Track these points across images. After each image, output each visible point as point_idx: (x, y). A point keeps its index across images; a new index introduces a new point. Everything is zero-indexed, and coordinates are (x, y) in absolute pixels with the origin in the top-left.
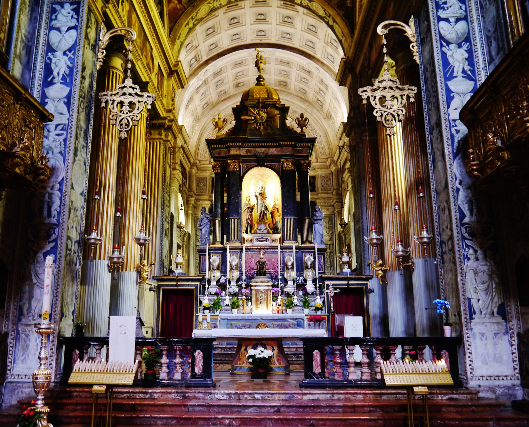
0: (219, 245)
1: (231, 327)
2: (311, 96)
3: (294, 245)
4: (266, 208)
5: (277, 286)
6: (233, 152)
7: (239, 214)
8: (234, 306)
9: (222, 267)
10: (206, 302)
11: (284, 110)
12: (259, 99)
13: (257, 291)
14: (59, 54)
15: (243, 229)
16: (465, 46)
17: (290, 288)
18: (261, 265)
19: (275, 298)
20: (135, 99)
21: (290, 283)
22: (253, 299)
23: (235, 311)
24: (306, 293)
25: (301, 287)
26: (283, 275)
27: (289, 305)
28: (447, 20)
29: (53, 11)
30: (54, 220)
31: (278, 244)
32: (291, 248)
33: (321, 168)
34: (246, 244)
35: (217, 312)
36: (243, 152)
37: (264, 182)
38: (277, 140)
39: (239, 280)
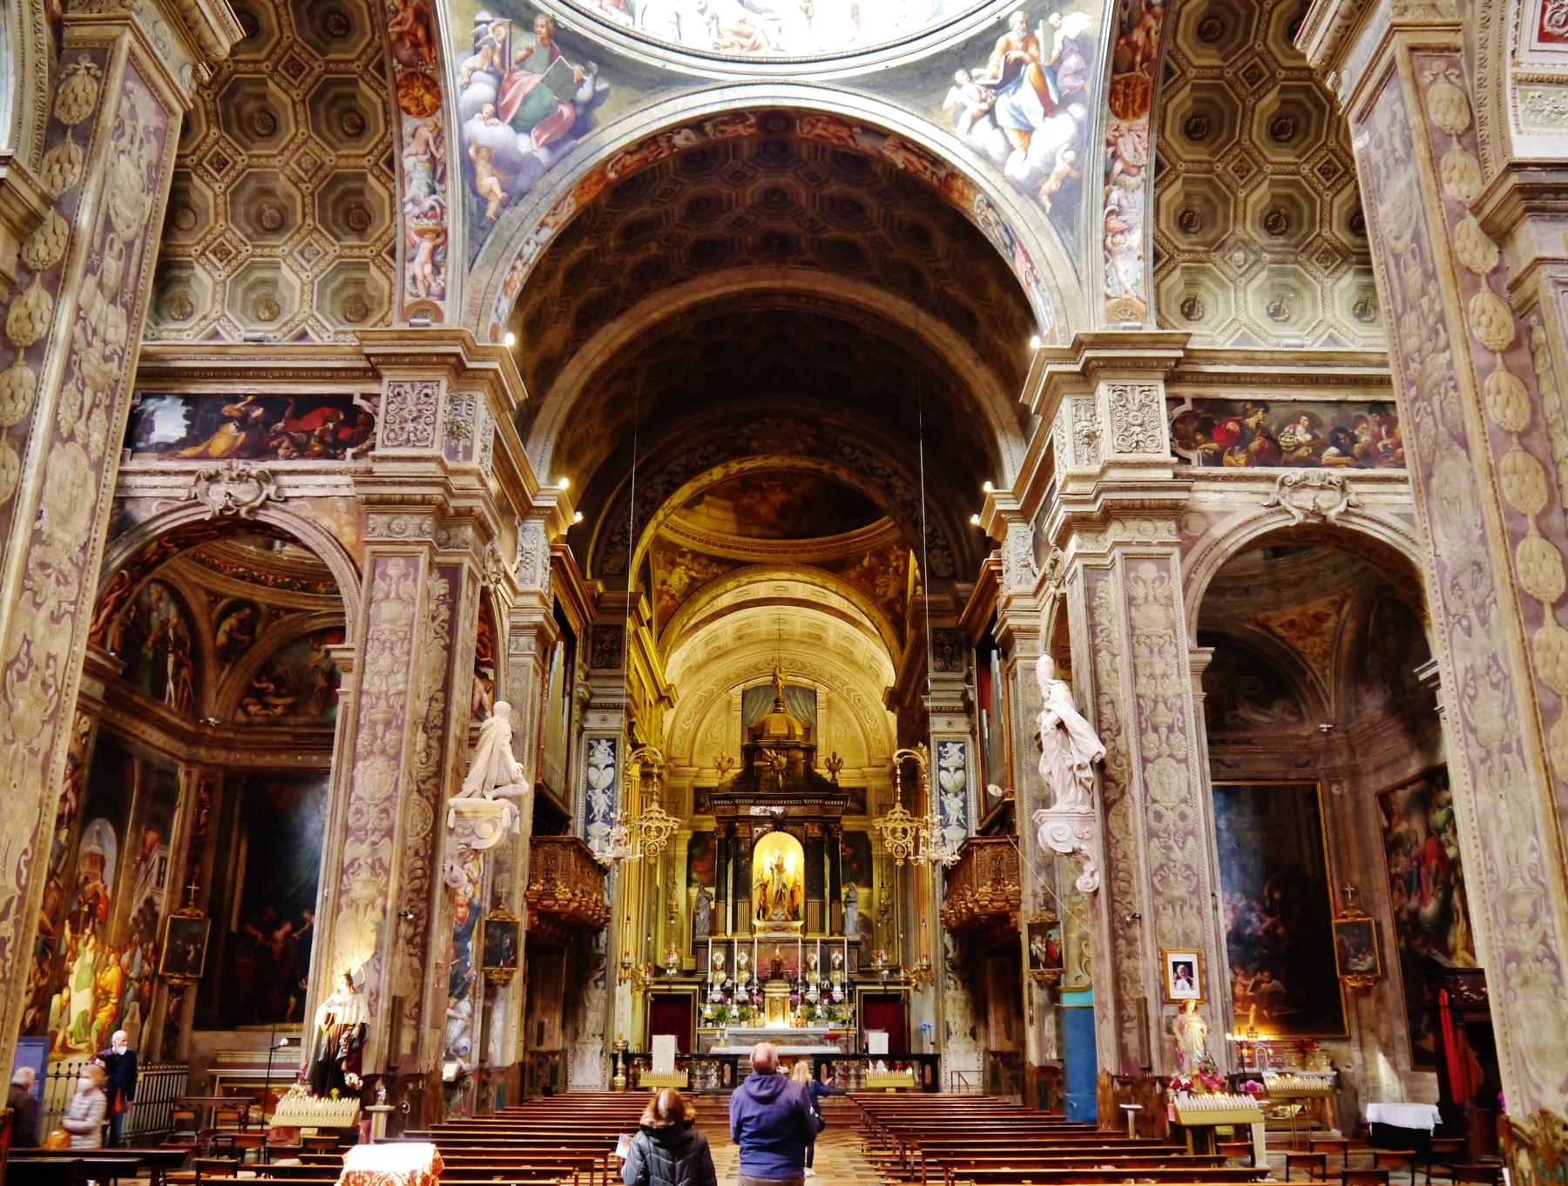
0: (722, 937)
1: (741, 1043)
2: (860, 658)
3: (818, 938)
4: (785, 886)
5: (796, 992)
6: (742, 812)
7: (749, 895)
8: (743, 1017)
9: (728, 966)
10: (708, 1012)
11: (811, 751)
12: (777, 737)
13: (772, 999)
14: (598, 791)
15: (755, 914)
16: (961, 795)
17: (813, 994)
18: (777, 965)
19: (793, 1006)
20: (662, 825)
21: (813, 988)
22: (767, 1009)
23: (744, 1024)
24: (832, 1002)
25: (826, 993)
26: (803, 978)
27: (811, 1017)
28: (947, 769)
29: (591, 747)
30: (602, 951)
31: (799, 935)
32: (814, 942)
33: (875, 776)
34: (758, 935)
35: (722, 1026)
36: (755, 811)
37: (782, 849)
38: (798, 798)
39: (747, 984)
